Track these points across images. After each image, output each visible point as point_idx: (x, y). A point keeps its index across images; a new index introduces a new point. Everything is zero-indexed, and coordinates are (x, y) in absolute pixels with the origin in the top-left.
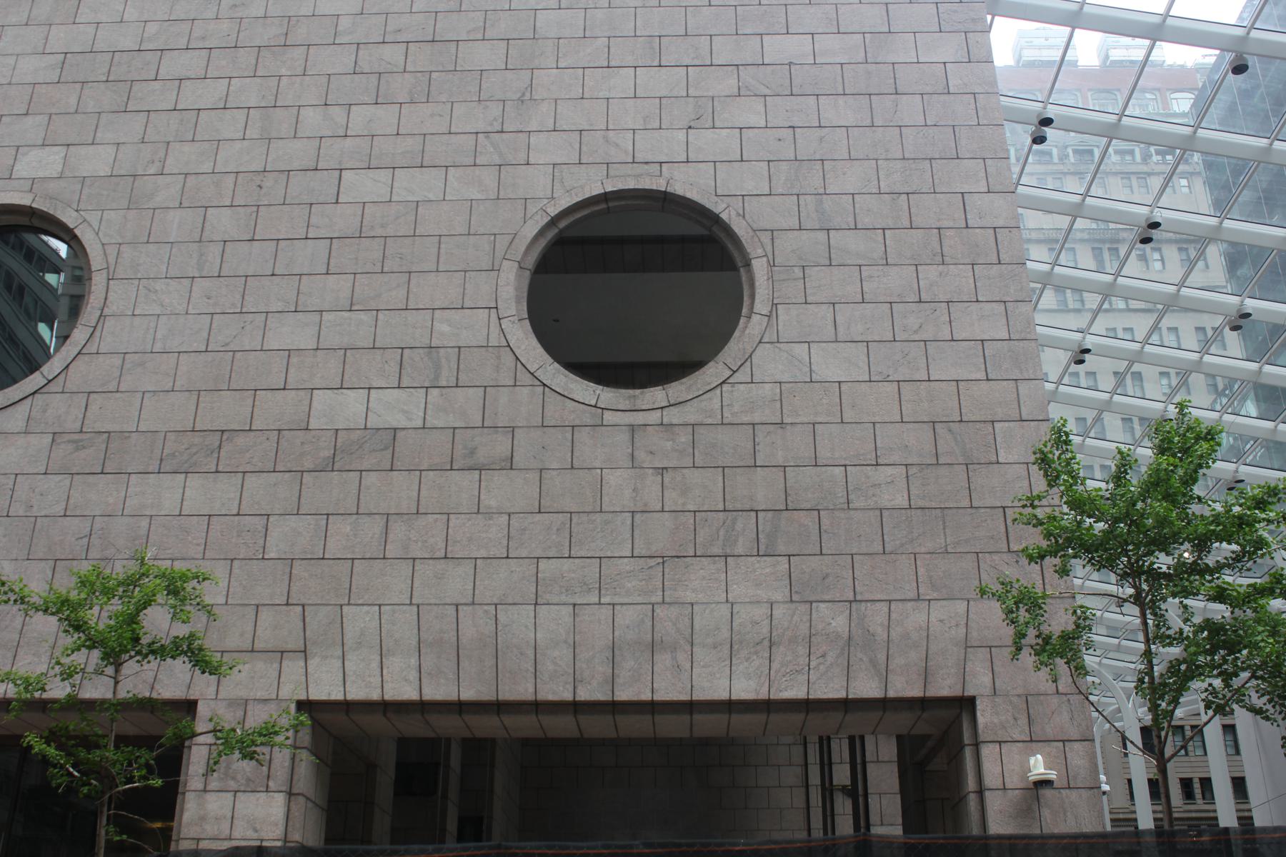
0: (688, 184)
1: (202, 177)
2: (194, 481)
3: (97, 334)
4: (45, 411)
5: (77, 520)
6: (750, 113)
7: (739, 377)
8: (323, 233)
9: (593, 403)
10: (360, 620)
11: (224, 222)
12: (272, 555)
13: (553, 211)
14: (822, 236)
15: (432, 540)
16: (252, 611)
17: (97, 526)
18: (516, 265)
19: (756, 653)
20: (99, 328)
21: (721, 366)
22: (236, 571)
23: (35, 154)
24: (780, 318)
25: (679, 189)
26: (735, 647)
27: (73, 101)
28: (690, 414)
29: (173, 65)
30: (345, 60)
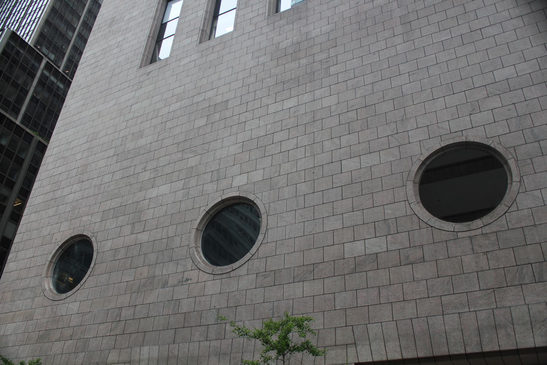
0: (474, 136)
1: (293, 174)
2: (306, 284)
3: (266, 236)
4: (253, 266)
5: (268, 304)
6: (495, 103)
7: (512, 209)
8: (338, 185)
9: (453, 230)
10: (374, 329)
11: (303, 188)
12: (338, 308)
13: (423, 159)
14: (536, 144)
15: (397, 294)
16: (333, 330)
17: (275, 305)
18: (412, 182)
19: (543, 325)
21: (503, 206)
22: (326, 315)
23: (238, 178)
24: (525, 181)
25: (471, 139)
26: (533, 323)
27: (248, 157)
28: (494, 228)
29: (278, 137)
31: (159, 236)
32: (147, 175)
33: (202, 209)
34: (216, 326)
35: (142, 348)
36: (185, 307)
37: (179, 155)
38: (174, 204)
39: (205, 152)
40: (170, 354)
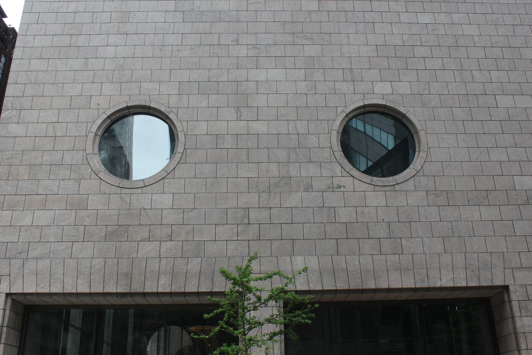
3: (429, 154)
4: (420, 183)
5: (445, 223)
8: (497, 118)
11: (460, 113)
12: (518, 234)
20: (429, 152)
30: (480, 54)
31: (284, 130)
32: (243, 51)
33: (340, 110)
34: (389, 240)
35: (293, 257)
36: (344, 215)
37: (290, 38)
38: (296, 95)
39: (327, 43)
40: (335, 266)
